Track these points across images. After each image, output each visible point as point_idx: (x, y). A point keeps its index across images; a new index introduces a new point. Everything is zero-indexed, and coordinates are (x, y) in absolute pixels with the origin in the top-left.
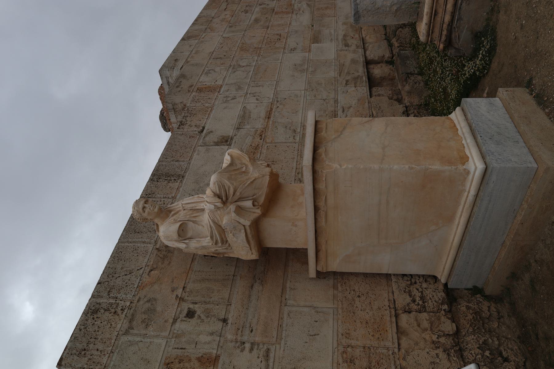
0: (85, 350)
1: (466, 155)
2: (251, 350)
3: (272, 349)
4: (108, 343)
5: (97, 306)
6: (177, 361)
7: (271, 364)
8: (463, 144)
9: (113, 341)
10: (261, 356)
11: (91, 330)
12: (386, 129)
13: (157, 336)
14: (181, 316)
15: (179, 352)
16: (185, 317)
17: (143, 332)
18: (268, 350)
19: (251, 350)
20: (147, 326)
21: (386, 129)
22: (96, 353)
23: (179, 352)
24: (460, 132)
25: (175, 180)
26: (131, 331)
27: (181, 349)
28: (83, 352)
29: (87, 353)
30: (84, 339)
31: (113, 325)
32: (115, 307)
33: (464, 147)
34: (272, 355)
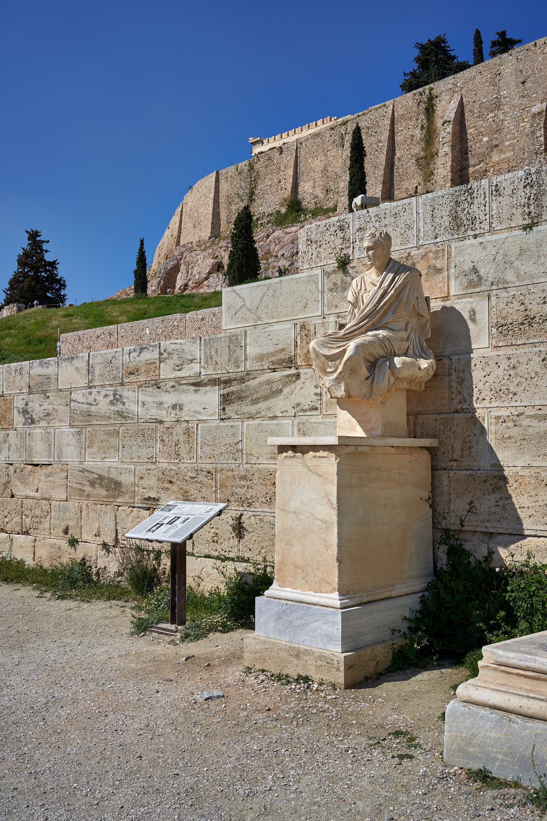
0: (312, 242)
1: (285, 587)
2: (316, 394)
3: (318, 412)
4: (318, 260)
5: (347, 226)
6: (307, 332)
7: (307, 413)
8: (297, 589)
9: (320, 264)
10: (313, 404)
11: (327, 235)
12: (319, 520)
13: (323, 305)
14: (340, 319)
15: (312, 332)
16: (339, 324)
17: (326, 289)
18: (316, 409)
19: (316, 394)
20: (331, 290)
21: (319, 520)
22: (310, 253)
23: (312, 332)
24: (312, 593)
25: (530, 212)
26: (326, 277)
27: (315, 332)
28: (309, 242)
29: (309, 247)
30: (319, 235)
31: (331, 255)
32: (347, 245)
33: (293, 589)
34: (314, 413)
